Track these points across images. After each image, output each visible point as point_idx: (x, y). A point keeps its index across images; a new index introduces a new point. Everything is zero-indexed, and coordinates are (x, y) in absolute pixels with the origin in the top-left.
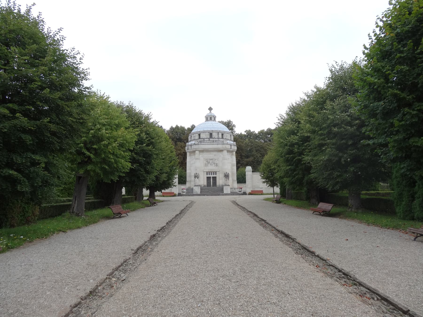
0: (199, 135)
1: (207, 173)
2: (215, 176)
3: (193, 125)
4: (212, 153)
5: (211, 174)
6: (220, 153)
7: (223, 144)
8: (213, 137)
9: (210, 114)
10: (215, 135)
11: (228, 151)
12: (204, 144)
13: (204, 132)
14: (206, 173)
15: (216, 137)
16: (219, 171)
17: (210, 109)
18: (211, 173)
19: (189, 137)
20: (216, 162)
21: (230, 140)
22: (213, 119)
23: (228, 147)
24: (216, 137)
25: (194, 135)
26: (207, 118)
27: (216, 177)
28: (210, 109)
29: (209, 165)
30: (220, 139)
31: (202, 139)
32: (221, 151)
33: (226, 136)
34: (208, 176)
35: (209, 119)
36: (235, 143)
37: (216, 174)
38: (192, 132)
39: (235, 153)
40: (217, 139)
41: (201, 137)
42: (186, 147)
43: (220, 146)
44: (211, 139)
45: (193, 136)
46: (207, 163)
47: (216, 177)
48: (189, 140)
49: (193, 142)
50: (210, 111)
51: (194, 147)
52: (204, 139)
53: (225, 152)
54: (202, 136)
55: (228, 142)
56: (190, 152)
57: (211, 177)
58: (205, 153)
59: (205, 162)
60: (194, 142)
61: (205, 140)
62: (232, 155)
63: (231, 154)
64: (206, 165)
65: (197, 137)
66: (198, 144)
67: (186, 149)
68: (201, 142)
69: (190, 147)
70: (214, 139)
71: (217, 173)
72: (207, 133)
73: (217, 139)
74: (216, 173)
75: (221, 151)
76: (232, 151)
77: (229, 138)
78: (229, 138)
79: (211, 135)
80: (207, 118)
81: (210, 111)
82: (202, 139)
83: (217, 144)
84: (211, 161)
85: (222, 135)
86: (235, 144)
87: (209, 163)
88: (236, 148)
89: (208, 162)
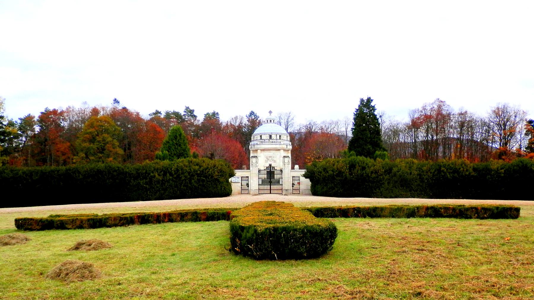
0: (261, 136)
3: (252, 111)
4: (271, 151)
6: (277, 152)
7: (280, 144)
8: (272, 138)
9: (270, 117)
10: (274, 137)
11: (284, 150)
12: (264, 144)
13: (265, 134)
15: (275, 138)
17: (270, 112)
19: (252, 137)
20: (274, 159)
21: (287, 140)
22: (272, 121)
23: (285, 146)
24: (275, 138)
25: (257, 136)
28: (270, 112)
29: (269, 161)
30: (278, 140)
31: (263, 140)
32: (279, 150)
33: (284, 137)
35: (269, 121)
36: (290, 143)
38: (254, 133)
39: (290, 151)
40: (275, 140)
41: (262, 139)
42: (250, 146)
43: (278, 146)
44: (270, 140)
45: (255, 136)
48: (252, 139)
49: (255, 142)
50: (270, 114)
51: (256, 147)
52: (265, 140)
53: (282, 151)
54: (263, 137)
55: (285, 142)
56: (253, 151)
58: (265, 152)
59: (265, 159)
60: (256, 143)
61: (266, 140)
62: (288, 153)
63: (287, 152)
64: (266, 162)
65: (259, 138)
66: (260, 144)
67: (250, 148)
68: (262, 142)
69: (253, 146)
70: (273, 140)
72: (267, 135)
73: (275, 140)
75: (279, 150)
76: (288, 150)
77: (286, 139)
78: (286, 139)
79: (270, 136)
81: (270, 114)
82: (263, 140)
83: (276, 144)
84: (270, 158)
85: (280, 136)
86: (291, 144)
87: (268, 159)
88: (290, 147)
89: (267, 159)
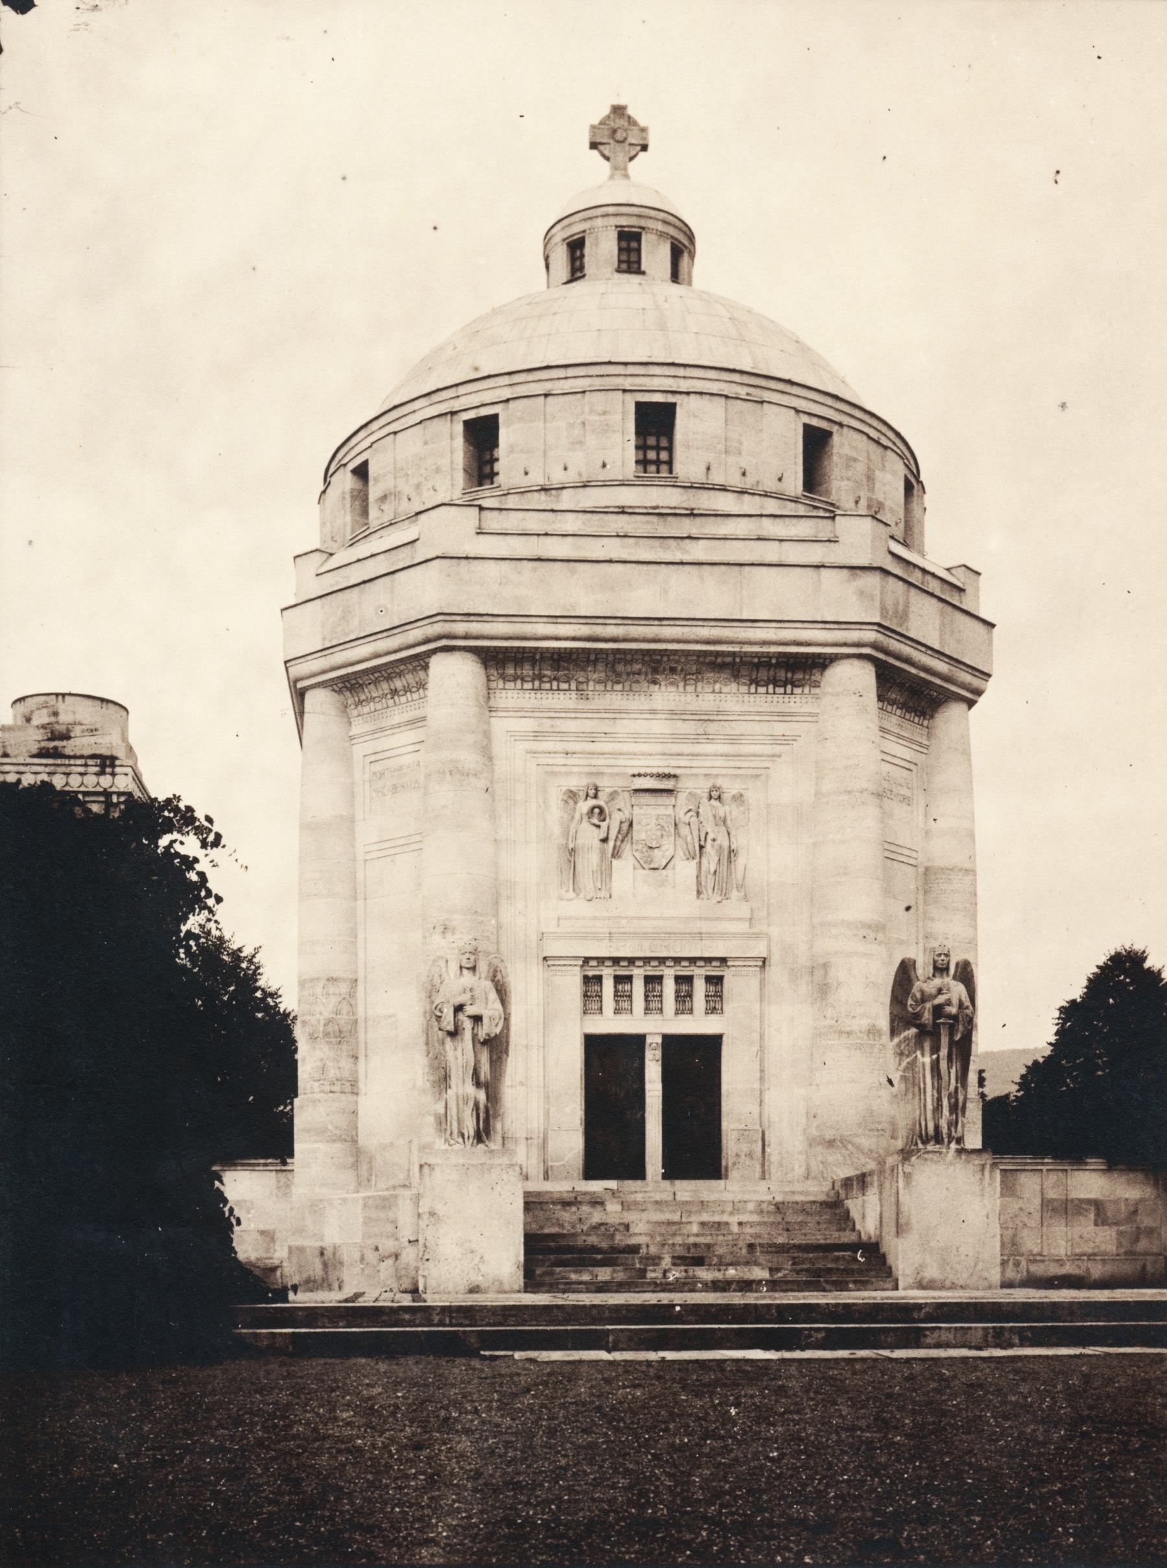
1: (592, 982)
2: (697, 1024)
5: (653, 1001)
8: (687, 464)
14: (571, 983)
16: (760, 950)
18: (653, 981)
22: (656, 256)
26: (576, 247)
27: (710, 1046)
34: (608, 1024)
37: (715, 1004)
46: (589, 836)
47: (710, 1046)
57: (654, 1041)
71: (735, 982)
74: (715, 981)
80: (576, 247)
